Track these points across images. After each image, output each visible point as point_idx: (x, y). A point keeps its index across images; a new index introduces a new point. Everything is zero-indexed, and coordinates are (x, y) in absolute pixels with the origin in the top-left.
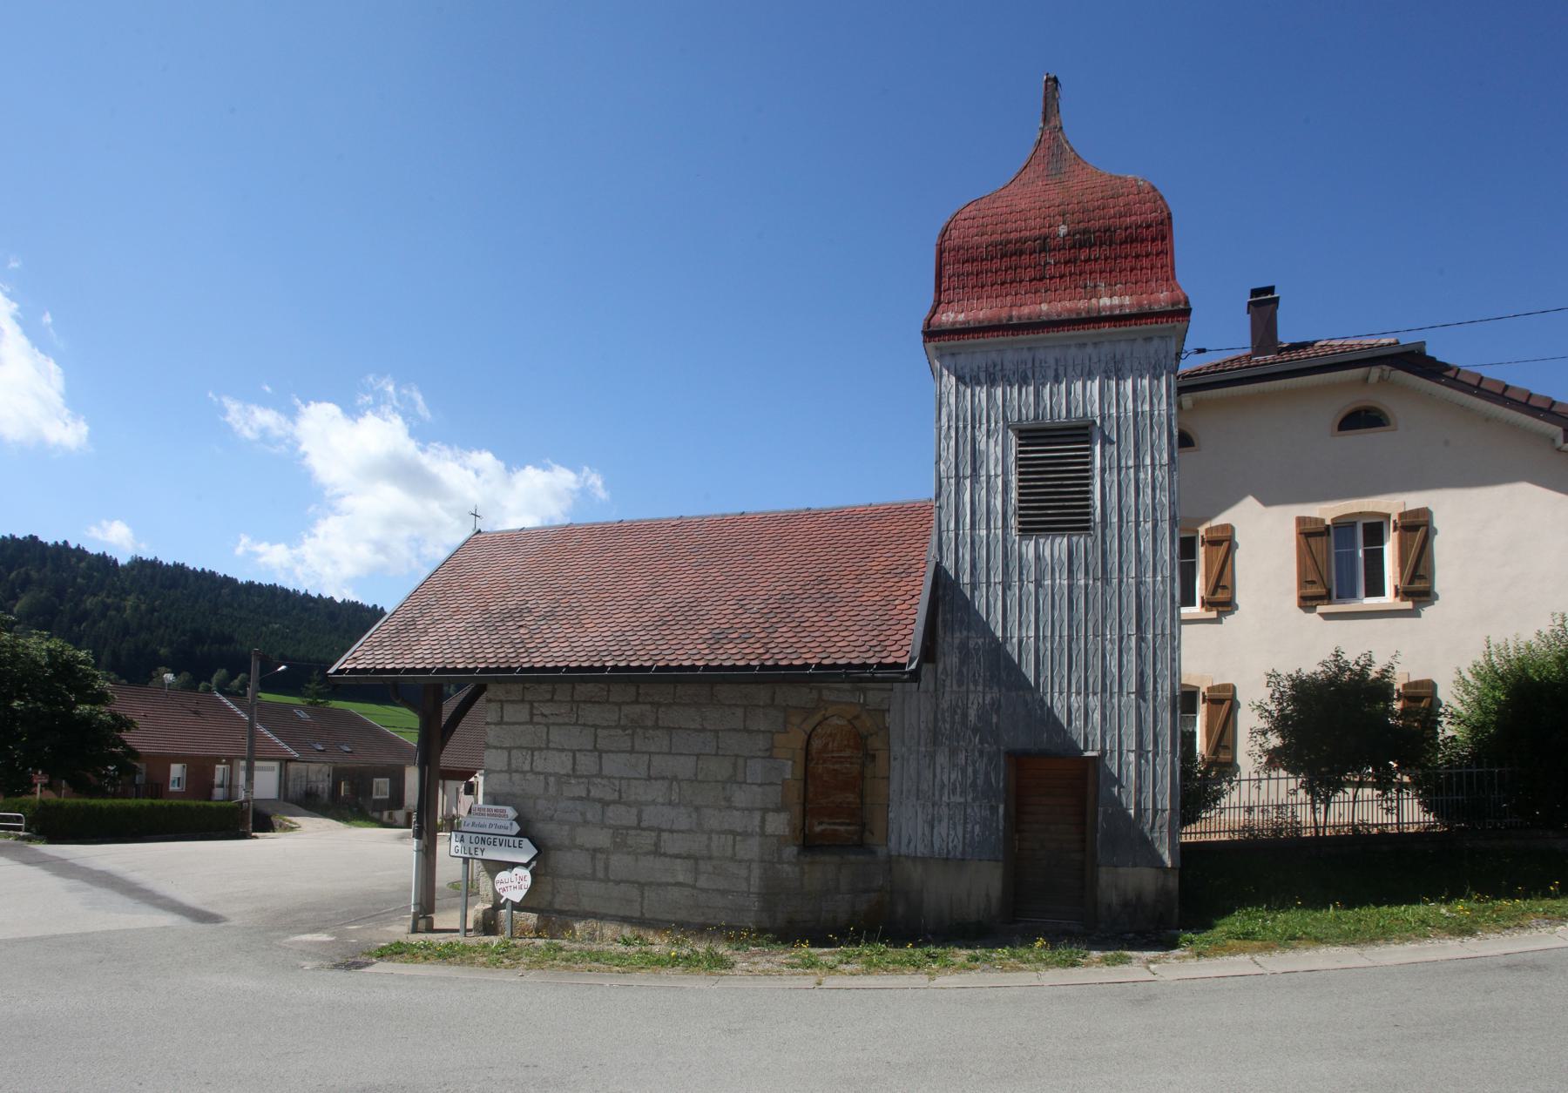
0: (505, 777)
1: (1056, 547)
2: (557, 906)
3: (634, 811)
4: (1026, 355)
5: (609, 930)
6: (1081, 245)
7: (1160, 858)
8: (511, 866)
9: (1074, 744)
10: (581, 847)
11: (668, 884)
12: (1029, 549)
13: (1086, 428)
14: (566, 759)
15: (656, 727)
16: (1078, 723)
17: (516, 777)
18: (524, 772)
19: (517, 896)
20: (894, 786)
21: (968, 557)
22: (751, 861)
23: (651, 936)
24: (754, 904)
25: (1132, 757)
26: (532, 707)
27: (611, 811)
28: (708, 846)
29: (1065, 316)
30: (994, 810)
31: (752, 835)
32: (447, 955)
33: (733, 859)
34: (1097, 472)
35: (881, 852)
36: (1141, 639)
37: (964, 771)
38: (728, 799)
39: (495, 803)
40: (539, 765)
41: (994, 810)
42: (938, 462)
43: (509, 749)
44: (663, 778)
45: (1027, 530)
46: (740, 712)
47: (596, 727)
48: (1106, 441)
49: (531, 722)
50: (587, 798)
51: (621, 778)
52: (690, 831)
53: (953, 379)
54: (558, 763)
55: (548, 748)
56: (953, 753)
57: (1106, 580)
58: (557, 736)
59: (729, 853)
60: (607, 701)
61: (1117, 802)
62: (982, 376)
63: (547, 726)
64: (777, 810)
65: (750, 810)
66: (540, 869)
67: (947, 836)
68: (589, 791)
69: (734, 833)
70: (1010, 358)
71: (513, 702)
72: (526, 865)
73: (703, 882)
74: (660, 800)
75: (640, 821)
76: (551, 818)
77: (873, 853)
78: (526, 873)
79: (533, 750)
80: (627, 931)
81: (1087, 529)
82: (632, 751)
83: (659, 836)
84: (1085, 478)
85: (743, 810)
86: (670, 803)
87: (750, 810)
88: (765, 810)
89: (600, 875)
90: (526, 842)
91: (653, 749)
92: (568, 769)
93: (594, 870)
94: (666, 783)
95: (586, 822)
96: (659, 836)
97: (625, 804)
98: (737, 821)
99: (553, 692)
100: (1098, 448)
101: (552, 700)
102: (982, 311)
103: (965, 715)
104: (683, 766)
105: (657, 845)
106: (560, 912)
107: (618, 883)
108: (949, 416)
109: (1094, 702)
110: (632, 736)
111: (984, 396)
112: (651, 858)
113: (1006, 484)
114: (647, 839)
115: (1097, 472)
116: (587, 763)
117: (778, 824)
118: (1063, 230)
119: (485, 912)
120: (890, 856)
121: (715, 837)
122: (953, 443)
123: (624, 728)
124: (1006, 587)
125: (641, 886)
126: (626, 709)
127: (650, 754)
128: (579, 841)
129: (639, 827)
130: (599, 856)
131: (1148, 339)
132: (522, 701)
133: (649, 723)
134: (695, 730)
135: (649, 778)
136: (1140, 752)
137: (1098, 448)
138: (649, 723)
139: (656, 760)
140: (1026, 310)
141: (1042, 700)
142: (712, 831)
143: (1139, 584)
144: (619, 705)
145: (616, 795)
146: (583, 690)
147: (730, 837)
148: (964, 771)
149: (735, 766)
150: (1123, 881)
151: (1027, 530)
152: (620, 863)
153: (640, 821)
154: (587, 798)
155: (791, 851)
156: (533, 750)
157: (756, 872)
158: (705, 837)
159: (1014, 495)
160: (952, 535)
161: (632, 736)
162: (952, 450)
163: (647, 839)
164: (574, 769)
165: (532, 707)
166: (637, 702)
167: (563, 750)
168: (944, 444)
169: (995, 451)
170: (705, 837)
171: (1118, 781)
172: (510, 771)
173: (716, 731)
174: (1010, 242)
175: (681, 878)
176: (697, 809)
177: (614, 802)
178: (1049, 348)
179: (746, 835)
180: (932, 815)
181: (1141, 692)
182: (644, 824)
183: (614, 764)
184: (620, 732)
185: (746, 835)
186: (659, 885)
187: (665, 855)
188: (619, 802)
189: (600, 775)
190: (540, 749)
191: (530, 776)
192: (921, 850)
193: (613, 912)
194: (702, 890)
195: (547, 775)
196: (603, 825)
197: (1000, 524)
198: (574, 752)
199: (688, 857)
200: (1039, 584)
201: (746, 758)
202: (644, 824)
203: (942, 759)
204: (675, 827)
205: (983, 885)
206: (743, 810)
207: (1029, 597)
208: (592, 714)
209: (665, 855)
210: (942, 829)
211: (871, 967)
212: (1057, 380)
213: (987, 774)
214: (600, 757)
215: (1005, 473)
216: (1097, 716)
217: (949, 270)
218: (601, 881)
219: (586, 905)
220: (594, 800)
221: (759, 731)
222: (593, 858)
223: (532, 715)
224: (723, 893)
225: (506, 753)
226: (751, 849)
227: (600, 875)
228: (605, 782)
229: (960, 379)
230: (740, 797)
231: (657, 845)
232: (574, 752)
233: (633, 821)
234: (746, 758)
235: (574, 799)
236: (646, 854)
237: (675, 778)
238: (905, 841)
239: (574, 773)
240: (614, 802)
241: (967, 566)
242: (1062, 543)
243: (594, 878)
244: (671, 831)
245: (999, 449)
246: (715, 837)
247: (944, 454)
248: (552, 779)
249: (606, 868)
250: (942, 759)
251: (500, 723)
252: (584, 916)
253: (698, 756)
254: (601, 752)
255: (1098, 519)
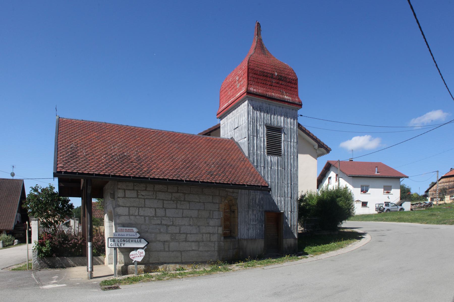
0: (127, 218)
1: (275, 159)
2: (151, 262)
3: (178, 228)
4: (268, 105)
5: (171, 266)
6: (280, 80)
7: (294, 236)
8: (136, 249)
9: (278, 209)
10: (159, 241)
11: (190, 250)
12: (269, 158)
13: (280, 129)
14: (153, 211)
15: (184, 201)
16: (279, 204)
17: (132, 217)
18: (136, 216)
19: (140, 259)
20: (239, 220)
21: (256, 158)
22: (215, 241)
23: (185, 267)
24: (216, 254)
25: (290, 212)
26: (138, 192)
27: (170, 229)
28: (202, 238)
29: (278, 98)
30: (262, 226)
31: (215, 234)
32: (135, 280)
33: (210, 241)
34: (283, 141)
35: (237, 239)
36: (291, 184)
37: (256, 216)
38: (208, 223)
39: (124, 227)
40: (142, 213)
41: (262, 226)
42: (248, 130)
43: (129, 207)
44: (187, 217)
45: (269, 154)
46: (211, 197)
47: (163, 200)
48: (285, 134)
49: (137, 197)
50: (161, 224)
51: (173, 217)
52: (197, 233)
53: (252, 107)
54: (149, 212)
55: (145, 207)
56: (253, 211)
57: (285, 169)
58: (148, 203)
59: (209, 239)
60: (167, 192)
61: (287, 223)
62: (258, 109)
63: (144, 199)
64: (220, 226)
65: (215, 226)
66: (147, 250)
67: (252, 233)
68: (161, 222)
69: (210, 233)
70: (265, 105)
71: (129, 190)
72: (142, 248)
73: (201, 249)
74: (187, 224)
75: (180, 231)
76: (147, 232)
77: (235, 238)
78: (143, 251)
79: (139, 208)
80: (178, 266)
81: (280, 155)
82: (177, 208)
83: (186, 236)
84: (280, 142)
85: (212, 226)
86: (190, 225)
87: (215, 226)
88: (218, 226)
89: (167, 249)
90: (142, 240)
91: (184, 208)
92: (153, 214)
93: (165, 248)
94: (189, 219)
95: (161, 233)
96: (186, 236)
97: (175, 226)
98: (211, 230)
99: (146, 187)
100: (283, 135)
101: (146, 190)
102: (260, 90)
103: (256, 201)
104: (194, 213)
105: (186, 238)
106: (152, 264)
107: (173, 252)
108: (251, 117)
109: (282, 199)
110: (176, 204)
111: (259, 114)
112: (184, 243)
113: (264, 140)
114: (183, 237)
115: (283, 141)
116: (160, 212)
117: (220, 230)
118: (276, 74)
119: (122, 267)
120: (238, 239)
121: (204, 235)
122: (252, 126)
123: (174, 201)
124: (264, 168)
125: (181, 252)
126: (174, 195)
127: (183, 209)
128: (158, 239)
129: (180, 233)
130: (166, 243)
131: (293, 110)
132: (134, 190)
133: (182, 199)
134: (198, 202)
135: (183, 217)
136: (291, 212)
137: (283, 135)
138: (182, 199)
139: (185, 211)
140: (270, 94)
141: (272, 198)
142: (203, 233)
143: (291, 171)
144: (172, 193)
145: (172, 223)
146: (158, 187)
147: (209, 235)
148: (256, 216)
149: (210, 213)
150: (288, 242)
151: (269, 154)
152: (173, 245)
153: (180, 231)
154: (161, 224)
155: (222, 238)
156: (139, 208)
157: (217, 244)
158: (201, 235)
159: (266, 143)
160: (252, 151)
161: (176, 204)
162: (252, 128)
163: (183, 237)
164: (155, 214)
165: (138, 192)
166: (177, 192)
167: (151, 208)
168: (249, 125)
169: (261, 130)
170: (201, 235)
171: (287, 218)
172: (129, 215)
173: (204, 203)
174: (265, 72)
175: (194, 248)
176: (199, 226)
177: (171, 225)
178: (274, 105)
179: (213, 234)
180: (249, 228)
181: (291, 198)
182: (181, 232)
183: (170, 213)
184: (172, 202)
185: (213, 234)
186: (187, 251)
187: (189, 241)
188: (173, 225)
189: (165, 216)
190: (142, 207)
191: (137, 217)
192: (246, 237)
193: (171, 261)
194: (201, 251)
195: (145, 217)
196: (167, 233)
197: (263, 150)
198: (155, 209)
199: (196, 242)
200: (271, 168)
201: (213, 211)
202: (181, 232)
203: (250, 212)
204: (192, 233)
205: (260, 245)
206: (212, 226)
207: (268, 170)
208: (161, 196)
209: (189, 241)
210: (251, 231)
211: (267, 264)
212: (275, 115)
213: (261, 216)
214: (165, 210)
215: (264, 137)
216: (283, 202)
217: (251, 75)
218: (167, 251)
219: (162, 260)
220: (164, 225)
221: (216, 203)
222: (164, 244)
223: (138, 195)
224: (208, 251)
225: (127, 209)
226: (215, 238)
227: (167, 249)
228: (167, 219)
229: (253, 108)
230: (212, 223)
231: (186, 238)
232: (155, 209)
233: (178, 231)
234: (213, 211)
235: (156, 224)
236: (183, 241)
237: (191, 217)
238: (242, 235)
239: (156, 216)
240: (171, 225)
241: (256, 161)
242: (276, 158)
243: (164, 251)
244: (191, 234)
245: (262, 130)
246: (204, 235)
247: (250, 128)
248: (147, 218)
249: (169, 247)
250: (250, 212)
251: (125, 197)
252: (162, 264)
253: (198, 210)
254: (165, 209)
255: (283, 153)
